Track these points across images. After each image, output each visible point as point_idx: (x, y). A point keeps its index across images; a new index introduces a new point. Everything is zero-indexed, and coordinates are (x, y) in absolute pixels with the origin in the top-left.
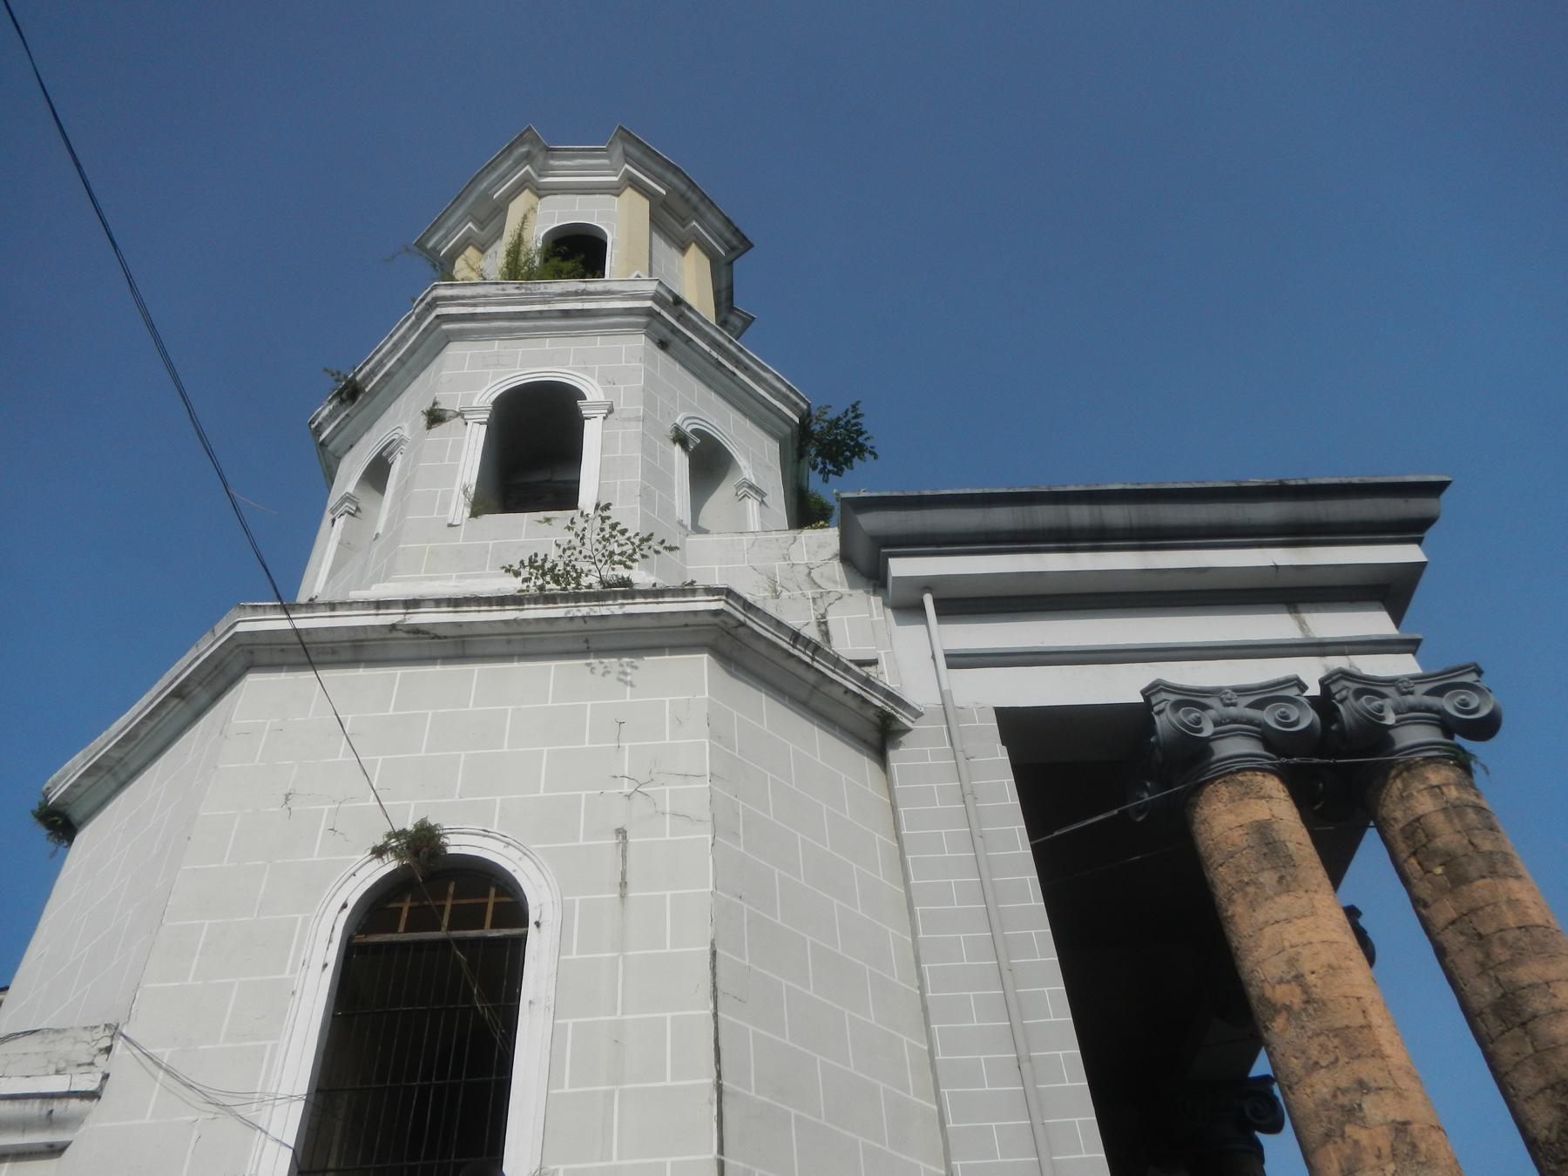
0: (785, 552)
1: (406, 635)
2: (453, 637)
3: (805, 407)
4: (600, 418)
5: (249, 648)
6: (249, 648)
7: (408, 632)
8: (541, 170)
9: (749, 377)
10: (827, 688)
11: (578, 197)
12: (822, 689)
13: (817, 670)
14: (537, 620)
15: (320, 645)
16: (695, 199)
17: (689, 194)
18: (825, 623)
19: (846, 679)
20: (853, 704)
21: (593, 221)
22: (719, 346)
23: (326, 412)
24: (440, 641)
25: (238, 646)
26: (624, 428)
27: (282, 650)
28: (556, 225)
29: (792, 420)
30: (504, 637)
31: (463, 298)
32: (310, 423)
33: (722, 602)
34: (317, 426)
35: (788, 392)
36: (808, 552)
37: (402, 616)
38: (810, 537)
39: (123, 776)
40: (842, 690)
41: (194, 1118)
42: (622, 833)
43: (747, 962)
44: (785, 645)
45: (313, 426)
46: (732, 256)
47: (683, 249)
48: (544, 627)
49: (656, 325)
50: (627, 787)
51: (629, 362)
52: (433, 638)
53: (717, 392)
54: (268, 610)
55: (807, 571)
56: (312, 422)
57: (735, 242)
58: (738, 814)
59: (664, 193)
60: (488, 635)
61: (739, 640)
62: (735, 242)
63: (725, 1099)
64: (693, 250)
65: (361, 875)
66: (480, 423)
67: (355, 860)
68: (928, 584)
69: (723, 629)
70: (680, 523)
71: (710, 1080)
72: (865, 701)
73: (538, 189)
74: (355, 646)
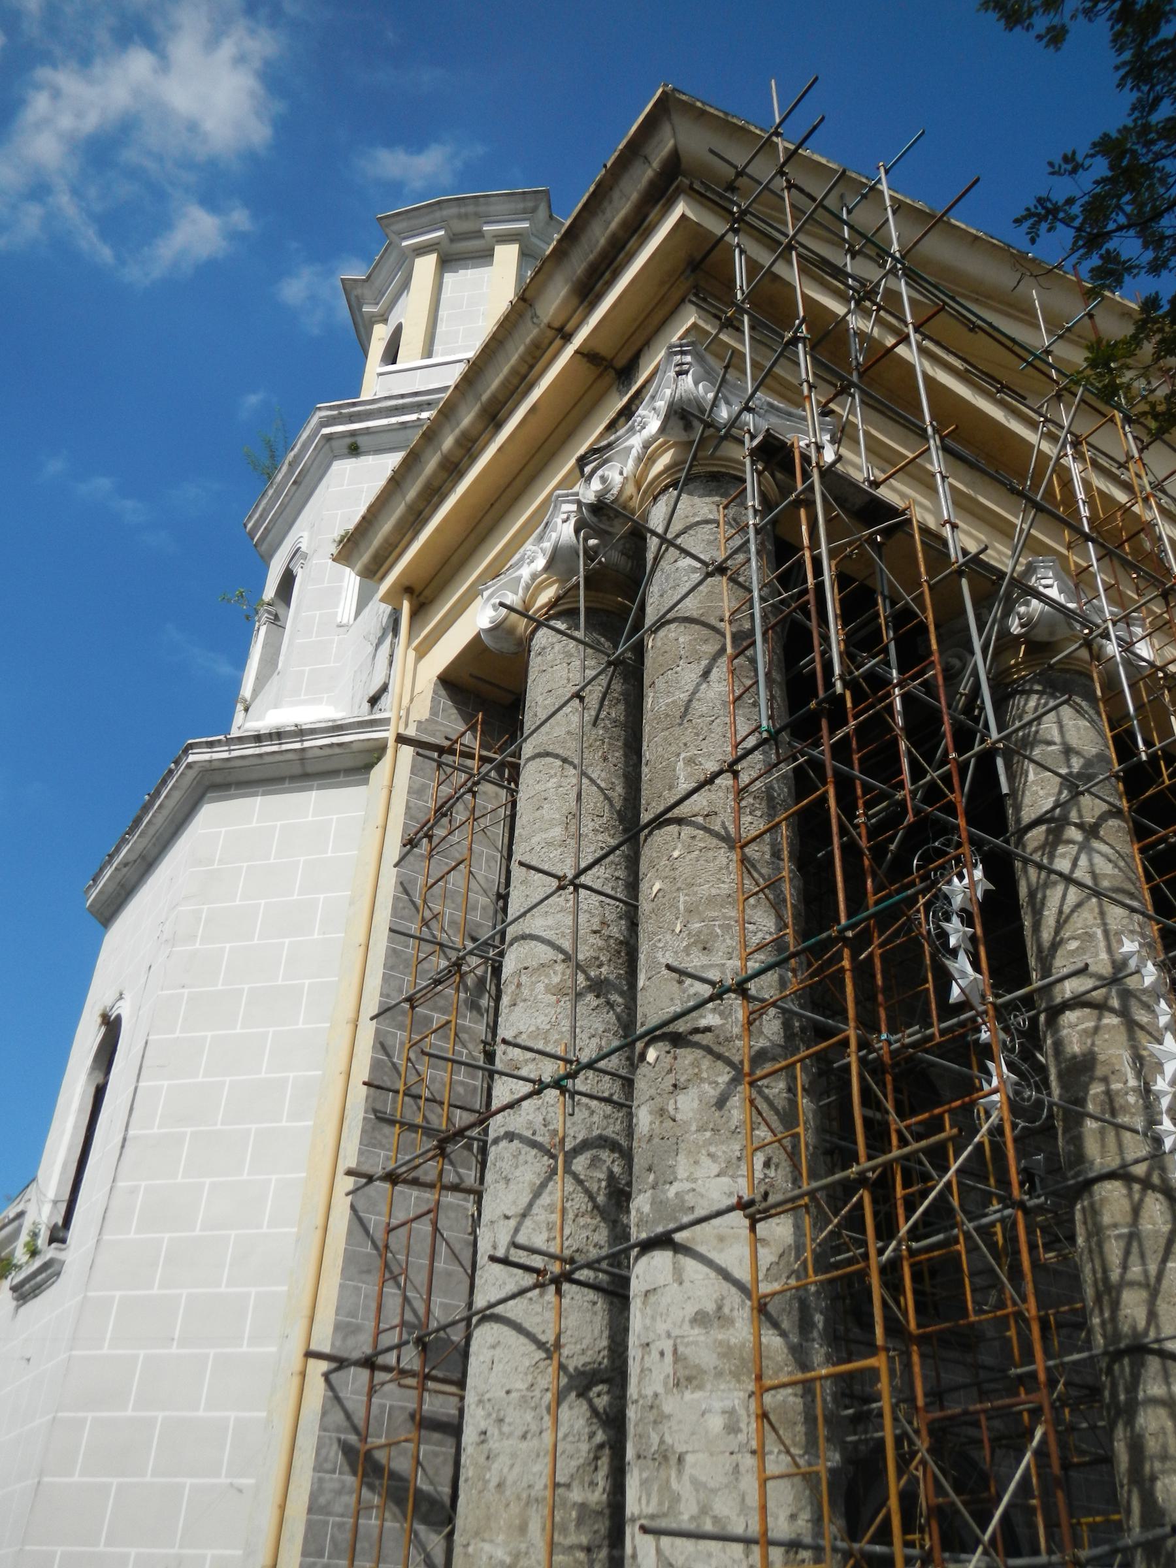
10: (309, 754)
16: (471, 209)
17: (463, 210)
20: (337, 750)
49: (335, 443)
57: (530, 204)
59: (442, 233)
63: (127, 1144)
72: (340, 745)
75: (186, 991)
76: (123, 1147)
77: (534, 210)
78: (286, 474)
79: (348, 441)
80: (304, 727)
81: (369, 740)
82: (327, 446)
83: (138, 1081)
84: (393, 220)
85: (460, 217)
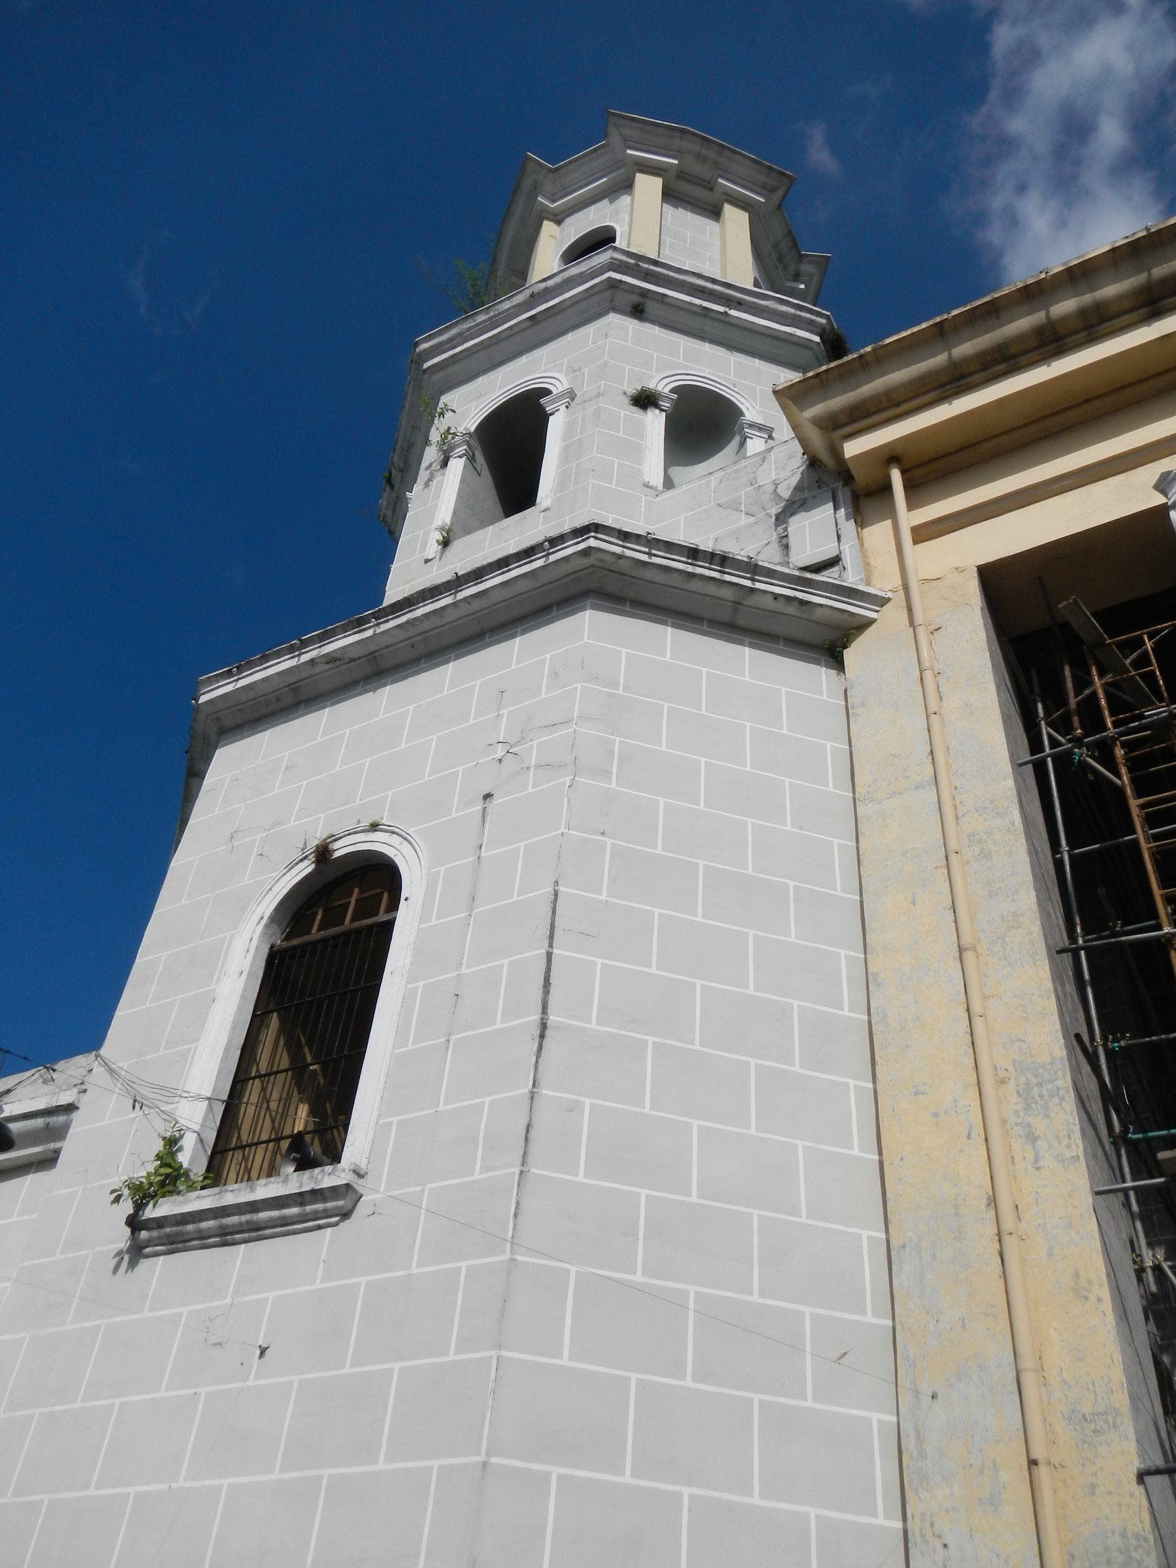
0: (752, 476)
2: (367, 656)
3: (824, 321)
4: (563, 408)
5: (215, 716)
6: (215, 716)
7: (327, 663)
8: (553, 195)
9: (746, 312)
10: (753, 601)
11: (593, 206)
12: (745, 603)
13: (730, 583)
14: (427, 616)
15: (265, 697)
17: (704, 152)
18: (786, 536)
19: (772, 584)
20: (791, 610)
21: (606, 222)
22: (702, 291)
27: (240, 710)
28: (573, 240)
29: (811, 341)
33: (592, 539)
34: (384, 518)
35: (798, 313)
36: (776, 468)
37: (318, 650)
38: (780, 452)
40: (769, 598)
42: (487, 796)
43: (604, 897)
44: (681, 566)
45: (381, 519)
46: (777, 197)
47: (714, 213)
48: (436, 622)
50: (500, 752)
51: (595, 343)
52: (349, 662)
53: (713, 341)
54: (219, 678)
55: (773, 487)
56: (379, 517)
57: (771, 182)
58: (612, 751)
60: (395, 644)
61: (628, 576)
62: (771, 182)
63: (548, 1033)
64: (728, 210)
65: (276, 889)
68: (891, 456)
69: (603, 568)
70: (647, 486)
71: (536, 1017)
72: (803, 603)
73: (556, 215)
74: (292, 690)
75: (609, 841)
76: (542, 1036)
77: (773, 190)
78: (518, 305)
79: (635, 299)
80: (760, 563)
81: (843, 611)
82: (609, 293)
83: (551, 945)
84: (626, 122)
85: (698, 156)
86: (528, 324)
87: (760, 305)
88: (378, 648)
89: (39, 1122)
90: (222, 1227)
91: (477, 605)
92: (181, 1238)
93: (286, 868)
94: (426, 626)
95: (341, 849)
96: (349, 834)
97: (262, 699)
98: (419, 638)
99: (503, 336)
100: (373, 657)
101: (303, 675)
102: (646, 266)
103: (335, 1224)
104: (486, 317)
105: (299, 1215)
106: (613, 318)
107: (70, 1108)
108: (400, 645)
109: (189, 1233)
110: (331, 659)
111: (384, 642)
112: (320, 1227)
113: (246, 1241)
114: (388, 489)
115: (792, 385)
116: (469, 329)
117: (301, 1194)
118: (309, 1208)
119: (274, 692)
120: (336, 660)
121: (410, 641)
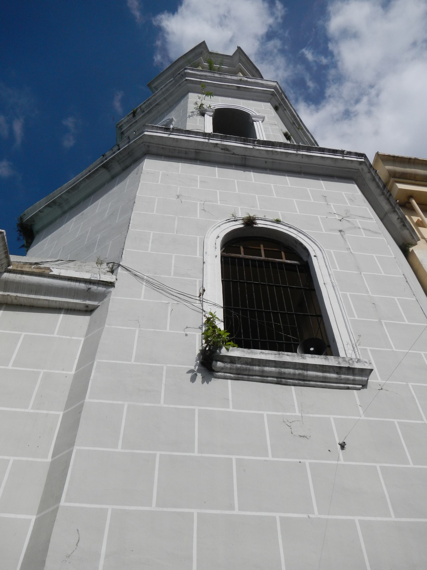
1: (221, 151)
2: (242, 155)
5: (148, 144)
7: (222, 149)
15: (180, 149)
23: (126, 120)
24: (235, 156)
25: (143, 143)
26: (271, 126)
27: (163, 148)
30: (264, 159)
31: (197, 75)
32: (118, 125)
34: (121, 126)
39: (66, 207)
41: (167, 302)
45: (118, 126)
52: (232, 154)
54: (158, 129)
66: (210, 116)
67: (218, 222)
73: (203, 67)
74: (196, 152)
78: (234, 80)
86: (235, 88)
87: (306, 133)
88: (249, 155)
89: (82, 286)
90: (280, 373)
91: (305, 160)
92: (247, 373)
93: (226, 220)
94: (277, 157)
95: (260, 224)
96: (262, 220)
97: (177, 149)
98: (271, 160)
99: (224, 86)
100: (245, 157)
101: (207, 148)
102: (283, 96)
103: (359, 389)
104: (219, 76)
105: (336, 378)
106: (269, 104)
107: (111, 285)
108: (260, 159)
109: (256, 371)
110: (226, 149)
111: (255, 154)
112: (348, 388)
113: (294, 385)
114: (131, 116)
115: (384, 155)
116: (210, 76)
117: (340, 368)
118: (343, 376)
119: (186, 148)
120: (227, 150)
121: (266, 160)
